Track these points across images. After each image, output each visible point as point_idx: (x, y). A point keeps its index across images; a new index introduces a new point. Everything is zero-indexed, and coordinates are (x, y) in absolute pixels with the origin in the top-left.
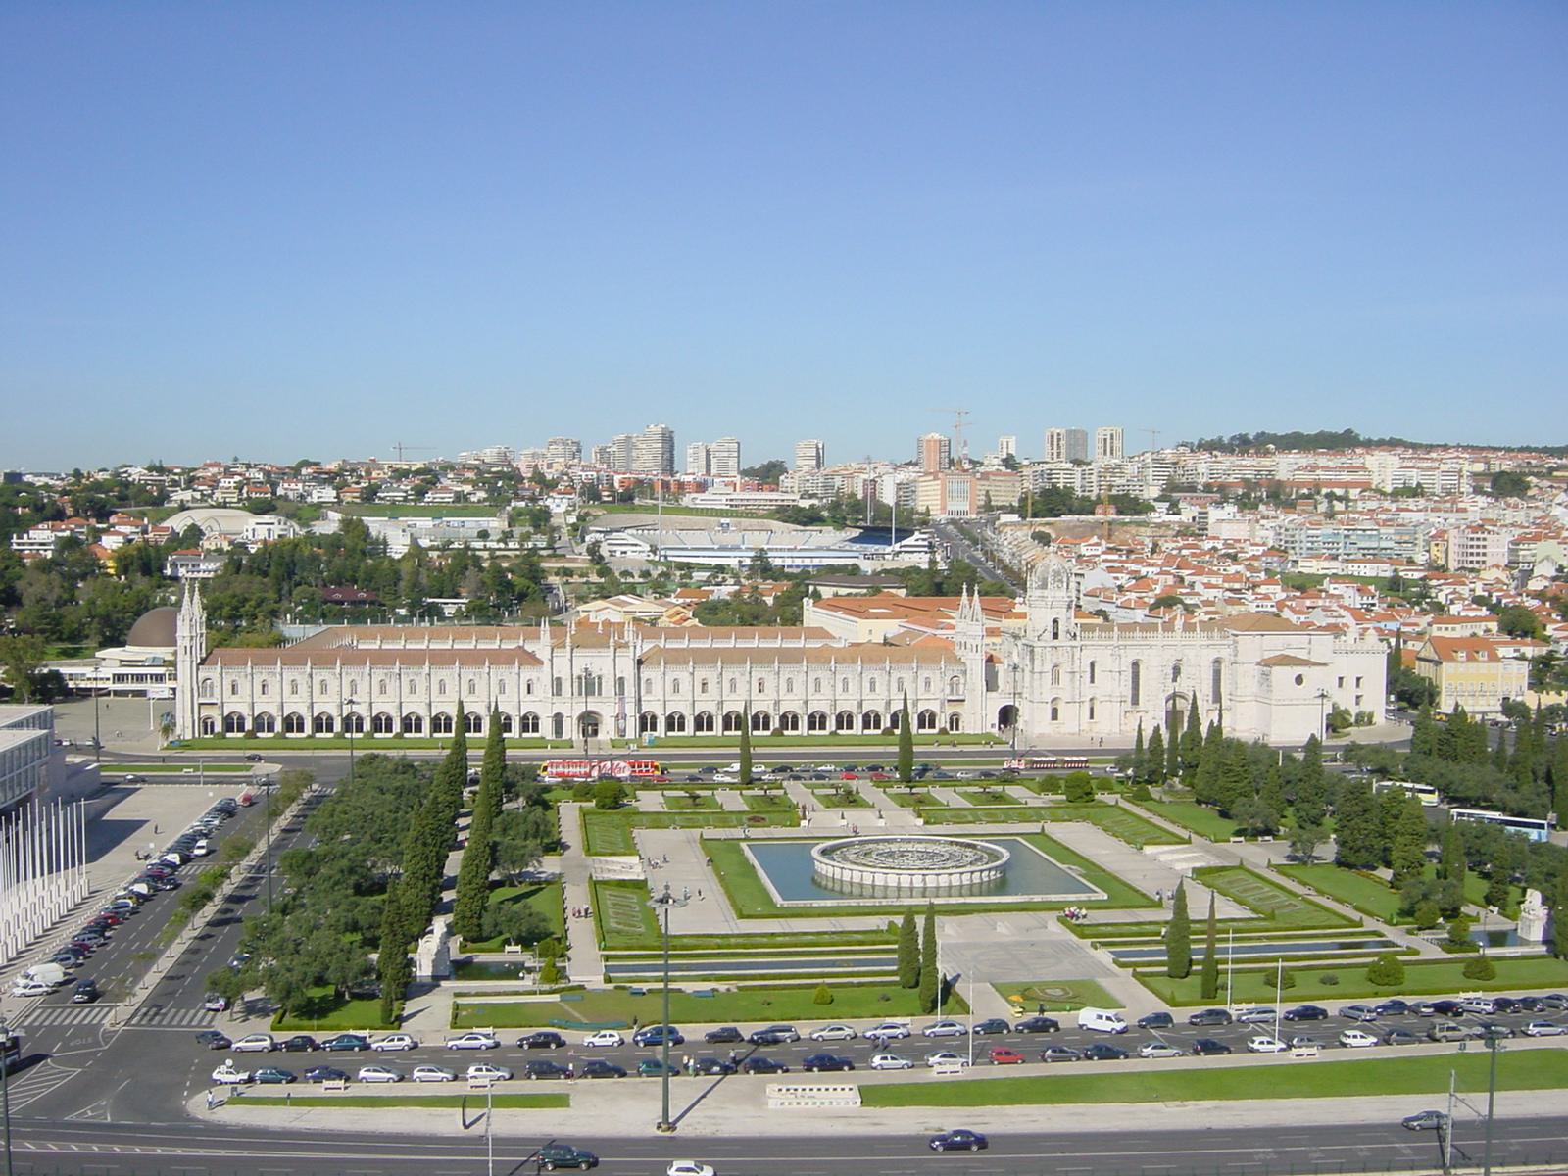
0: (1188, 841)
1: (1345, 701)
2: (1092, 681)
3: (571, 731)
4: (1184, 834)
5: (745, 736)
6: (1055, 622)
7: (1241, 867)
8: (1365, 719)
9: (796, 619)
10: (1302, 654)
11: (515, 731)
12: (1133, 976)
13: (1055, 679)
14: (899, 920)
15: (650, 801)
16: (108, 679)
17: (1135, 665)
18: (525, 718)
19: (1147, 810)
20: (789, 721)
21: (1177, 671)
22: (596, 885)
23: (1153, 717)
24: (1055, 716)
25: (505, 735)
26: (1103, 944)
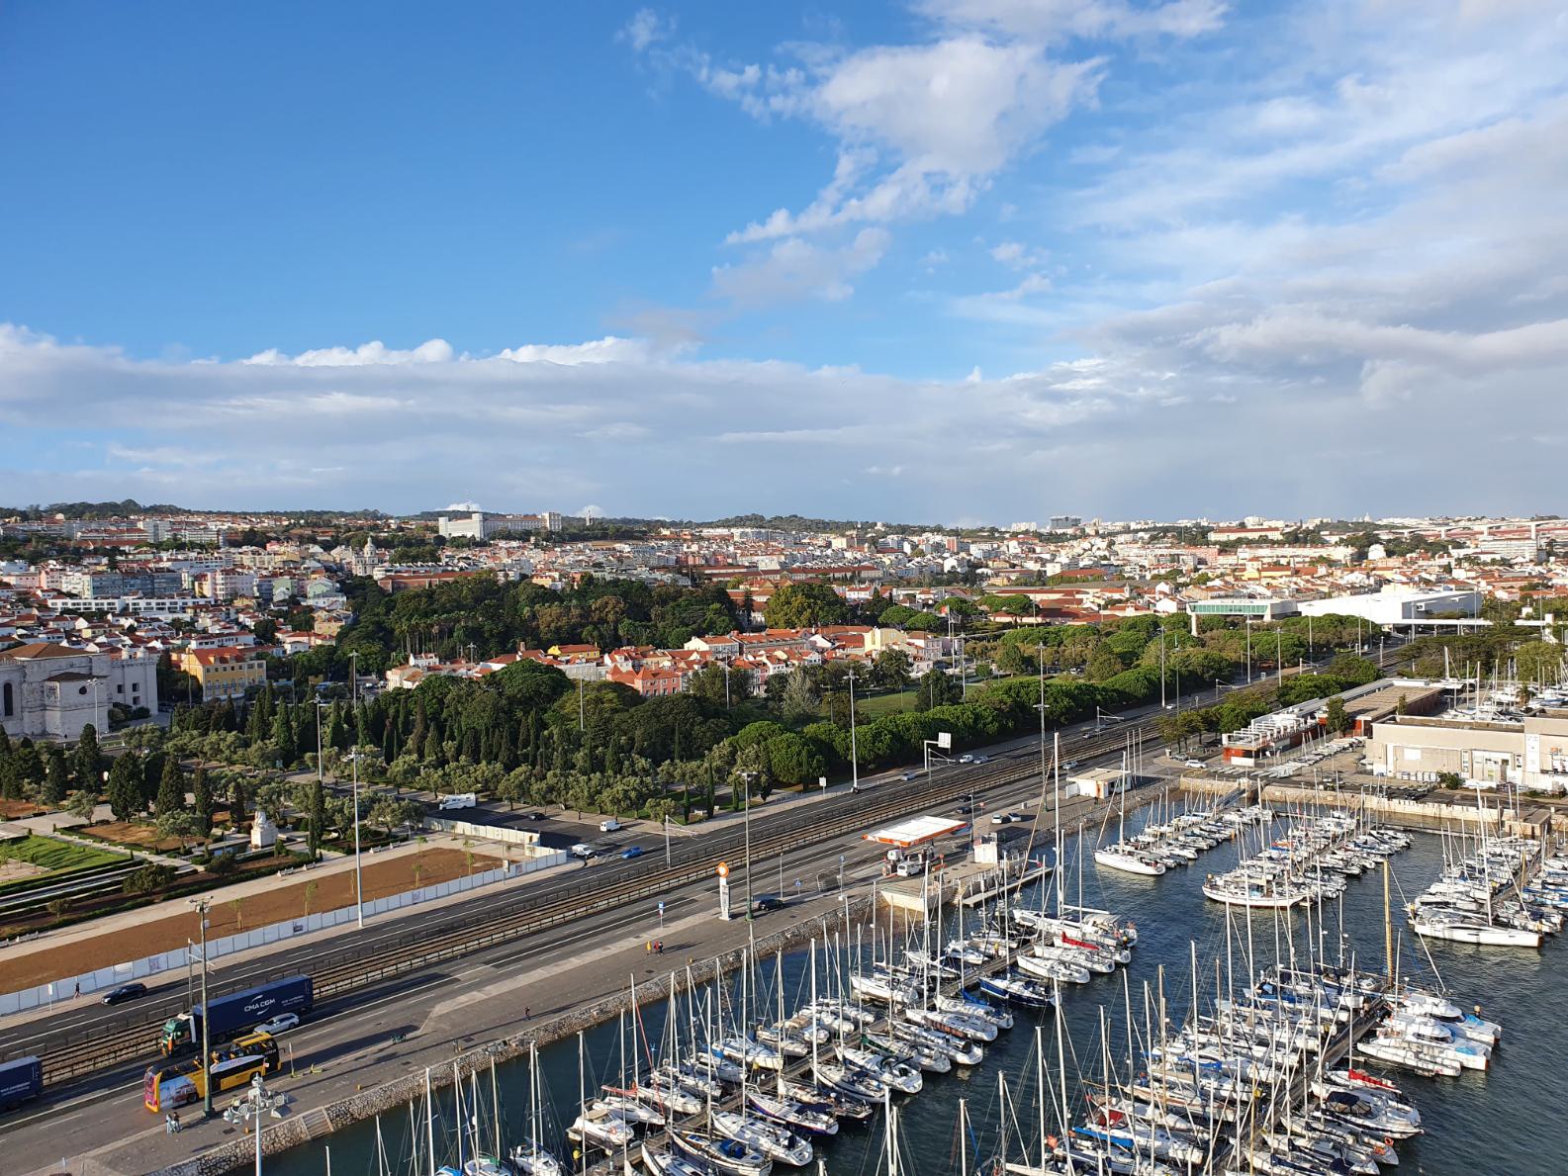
1: (127, 698)
8: (143, 714)
10: (83, 671)
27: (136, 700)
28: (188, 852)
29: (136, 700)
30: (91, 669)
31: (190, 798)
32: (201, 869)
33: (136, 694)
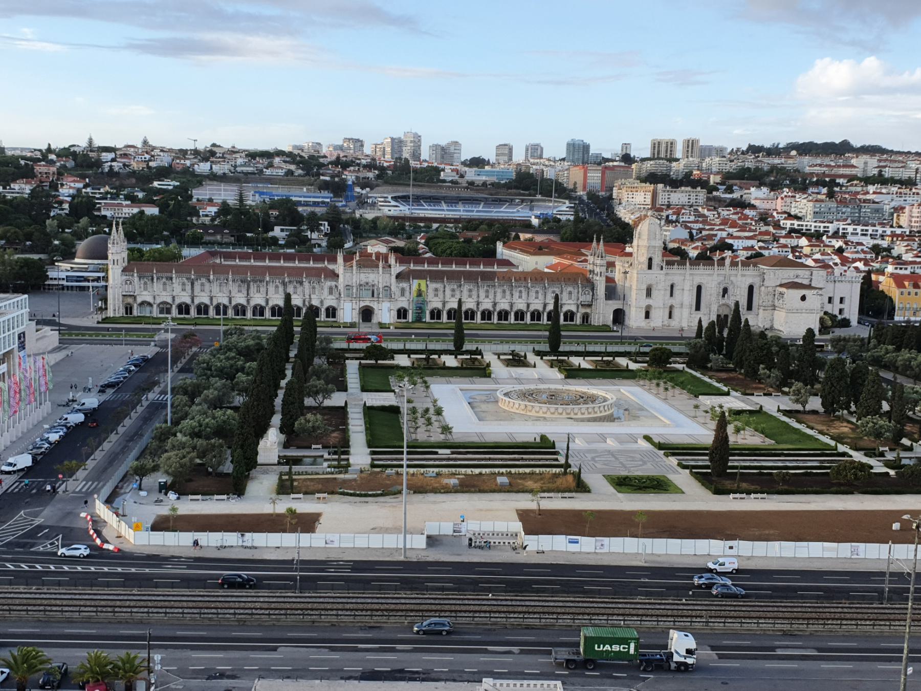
0: (728, 394)
2: (671, 295)
4: (726, 389)
6: (650, 260)
8: (845, 323)
9: (493, 253)
10: (806, 282)
11: (323, 317)
12: (691, 473)
16: (63, 279)
17: (699, 288)
18: (327, 309)
21: (725, 291)
22: (369, 412)
23: (708, 316)
24: (647, 315)
25: (317, 319)
26: (674, 454)
27: (841, 311)
28: (882, 454)
29: (841, 311)
30: (811, 281)
31: (886, 406)
32: (892, 473)
33: (842, 306)
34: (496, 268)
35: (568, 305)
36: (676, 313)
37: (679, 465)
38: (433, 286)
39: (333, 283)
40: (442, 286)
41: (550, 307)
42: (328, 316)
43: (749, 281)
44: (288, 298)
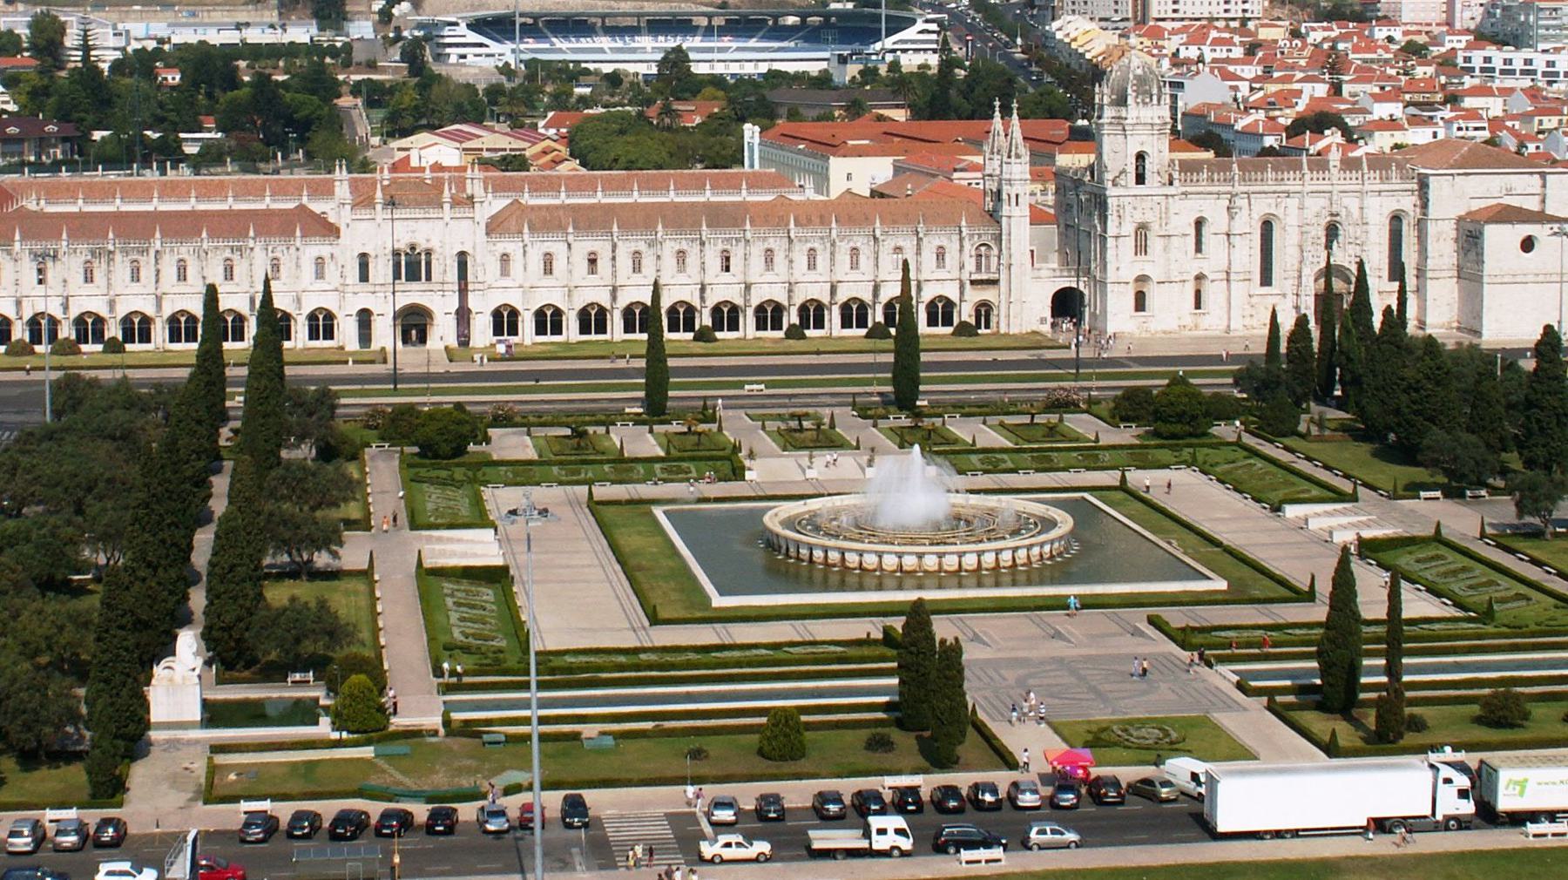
0: (1353, 498)
2: (1198, 249)
3: (384, 334)
4: (1347, 486)
5: (656, 344)
7: (1438, 538)
10: (1532, 204)
11: (299, 339)
12: (1271, 708)
13: (1141, 247)
14: (898, 623)
15: (511, 445)
17: (1267, 227)
18: (312, 317)
19: (1286, 448)
20: (727, 316)
21: (1332, 232)
22: (430, 577)
24: (1140, 302)
25: (287, 344)
26: (1223, 660)
30: (1543, 201)
34: (744, 196)
35: (936, 284)
36: (1213, 293)
37: (1240, 686)
38: (583, 246)
39: (324, 249)
40: (609, 246)
41: (892, 290)
42: (313, 335)
43: (1390, 205)
44: (211, 295)
